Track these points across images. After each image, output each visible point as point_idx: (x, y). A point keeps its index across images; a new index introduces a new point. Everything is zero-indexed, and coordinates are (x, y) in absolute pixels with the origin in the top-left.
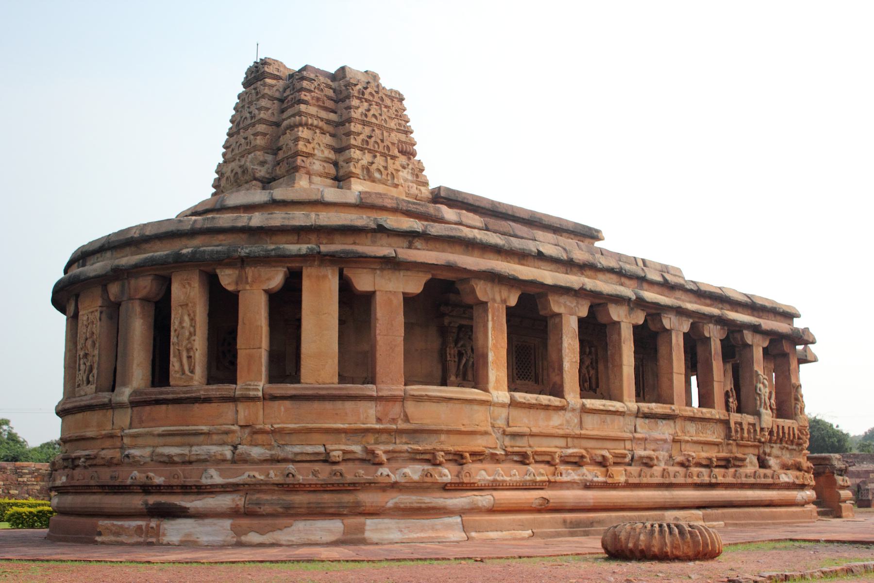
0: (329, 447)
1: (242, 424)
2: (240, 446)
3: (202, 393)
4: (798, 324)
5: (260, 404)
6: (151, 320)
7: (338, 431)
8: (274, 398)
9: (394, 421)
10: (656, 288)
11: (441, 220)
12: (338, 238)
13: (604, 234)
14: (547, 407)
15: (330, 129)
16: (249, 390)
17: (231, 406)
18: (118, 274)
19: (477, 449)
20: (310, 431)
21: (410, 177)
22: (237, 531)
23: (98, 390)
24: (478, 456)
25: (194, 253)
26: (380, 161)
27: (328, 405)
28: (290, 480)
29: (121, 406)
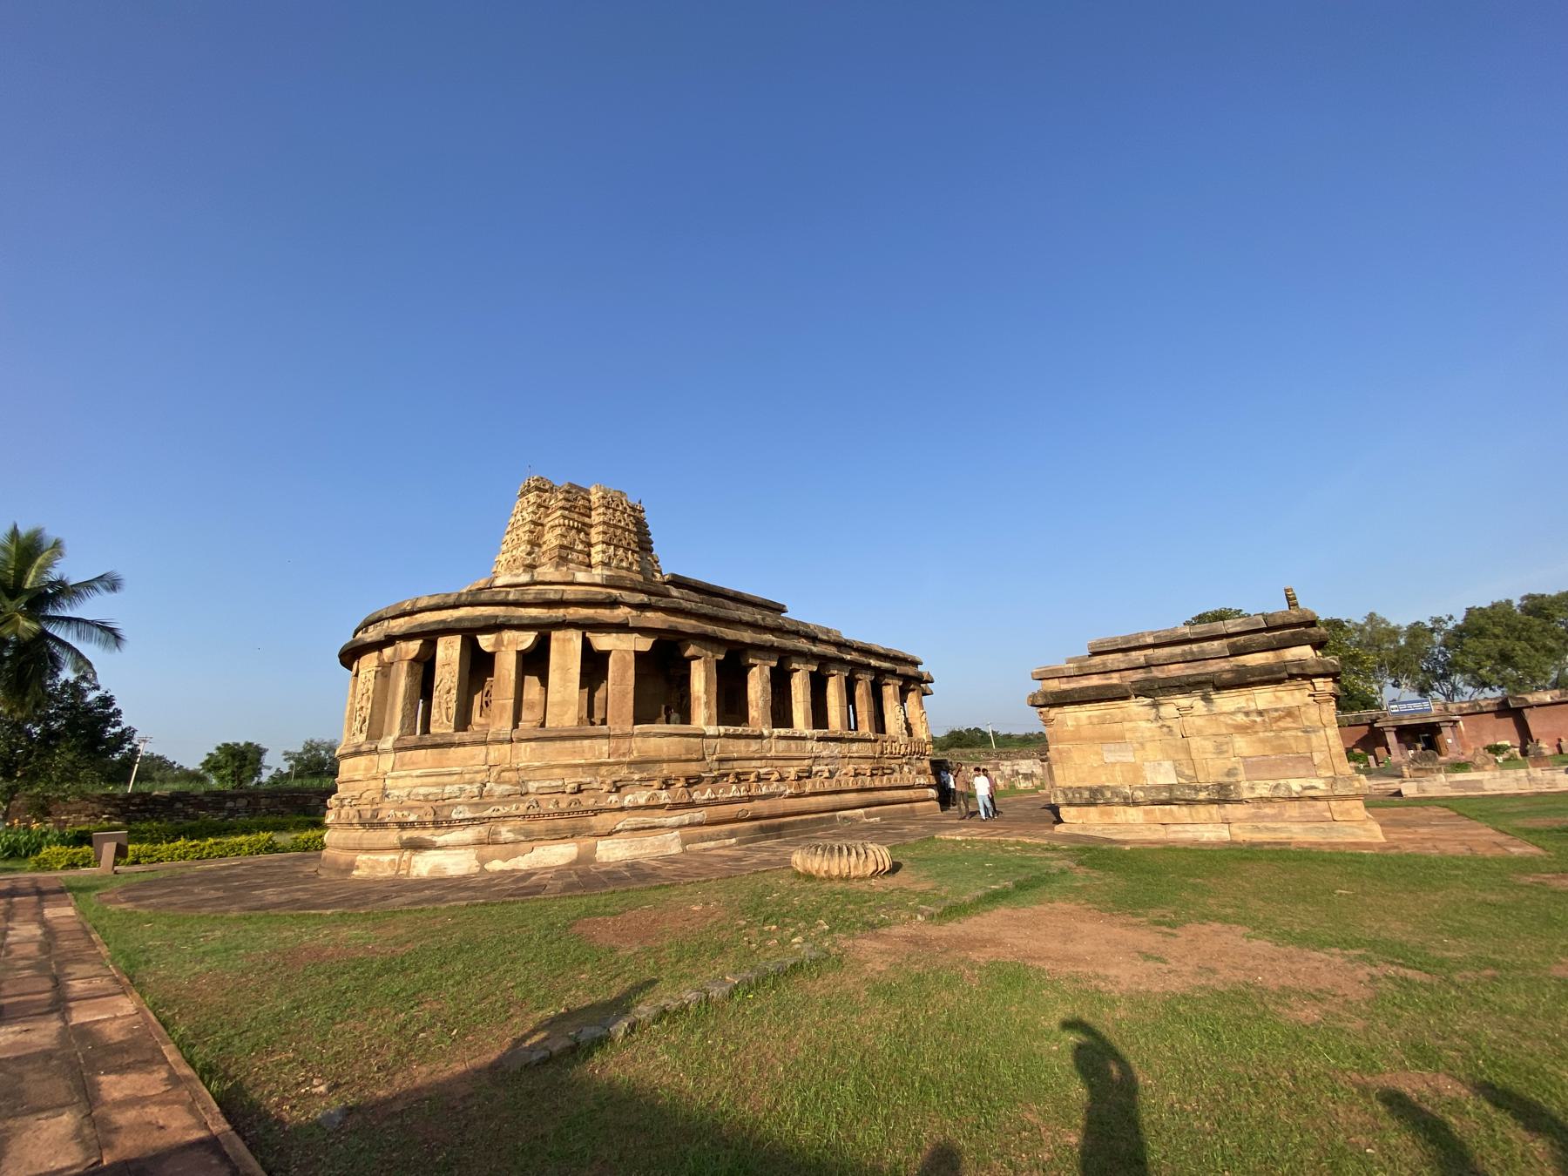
4: (920, 668)
5: (507, 747)
6: (419, 677)
7: (576, 766)
8: (521, 740)
9: (624, 755)
11: (669, 596)
14: (748, 737)
17: (484, 748)
18: (390, 640)
19: (693, 773)
20: (553, 767)
22: (483, 861)
23: (369, 737)
24: (692, 781)
27: (568, 744)
28: (531, 811)
29: (385, 751)
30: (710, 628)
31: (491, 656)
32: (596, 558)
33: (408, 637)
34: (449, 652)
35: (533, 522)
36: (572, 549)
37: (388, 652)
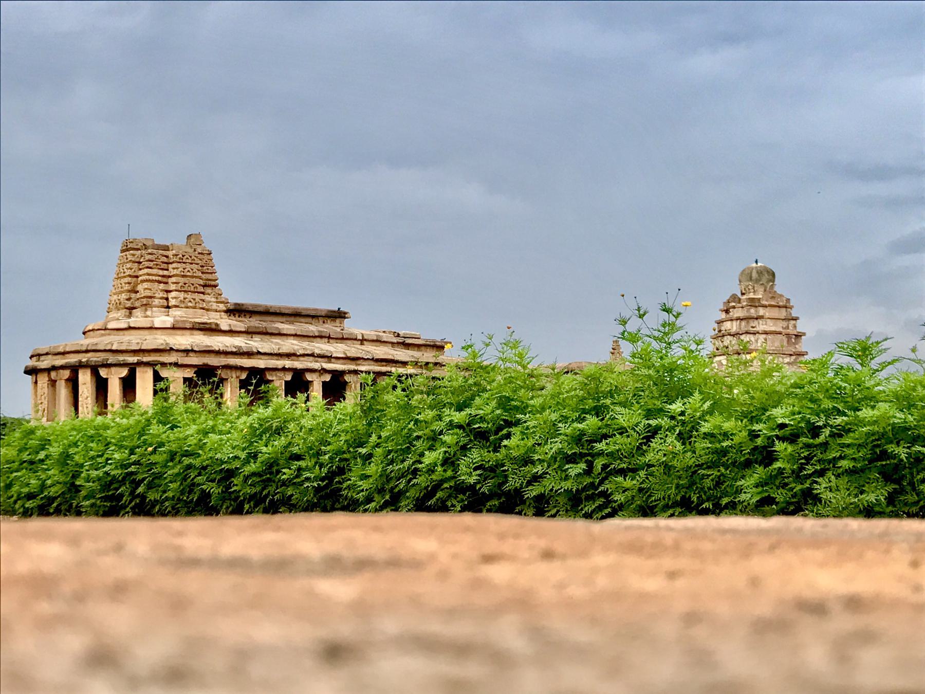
10: (342, 361)
12: (152, 354)
13: (351, 314)
15: (165, 280)
18: (54, 368)
21: (213, 300)
23: (48, 420)
25: (87, 361)
26: (189, 296)
30: (233, 361)
31: (106, 380)
32: (172, 302)
33: (63, 367)
34: (85, 377)
35: (130, 276)
36: (154, 297)
37: (53, 374)
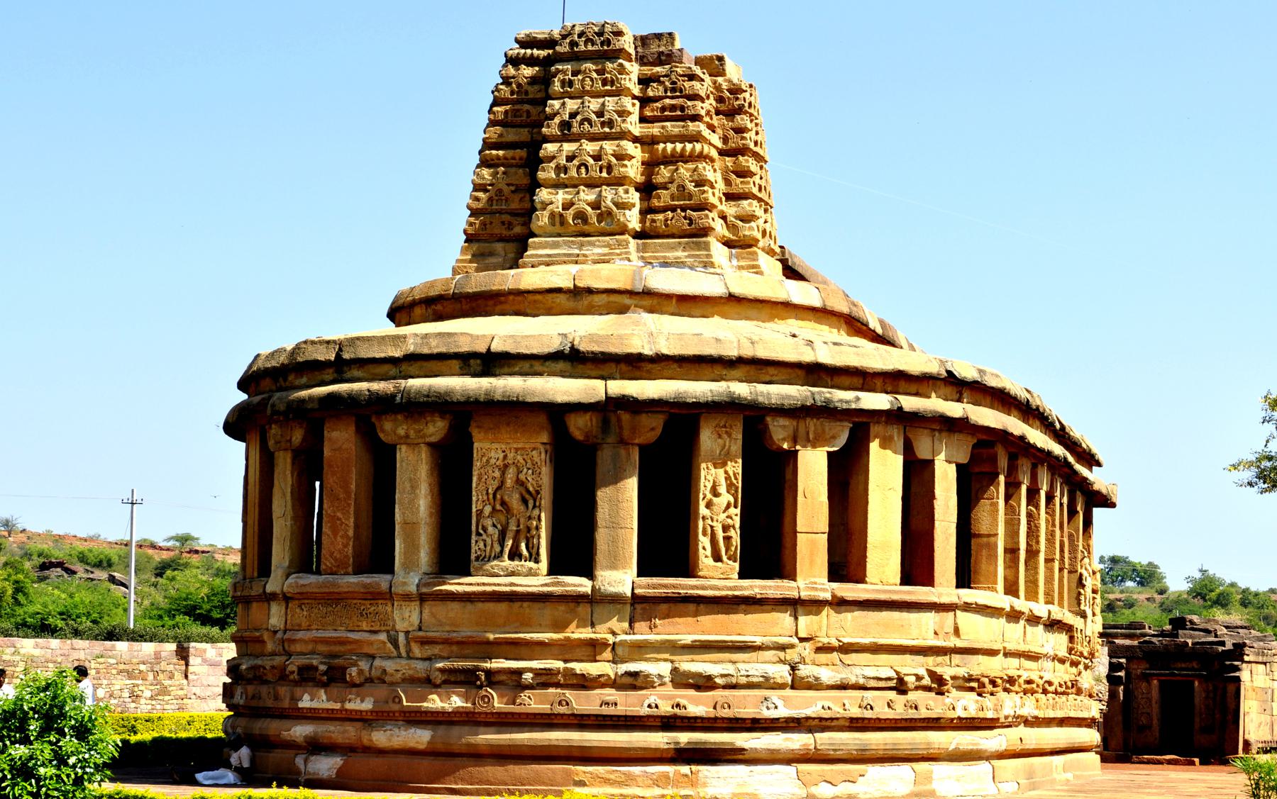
0: (903, 671)
1: (802, 635)
2: (801, 666)
3: (757, 590)
16: (816, 589)
28: (868, 714)
